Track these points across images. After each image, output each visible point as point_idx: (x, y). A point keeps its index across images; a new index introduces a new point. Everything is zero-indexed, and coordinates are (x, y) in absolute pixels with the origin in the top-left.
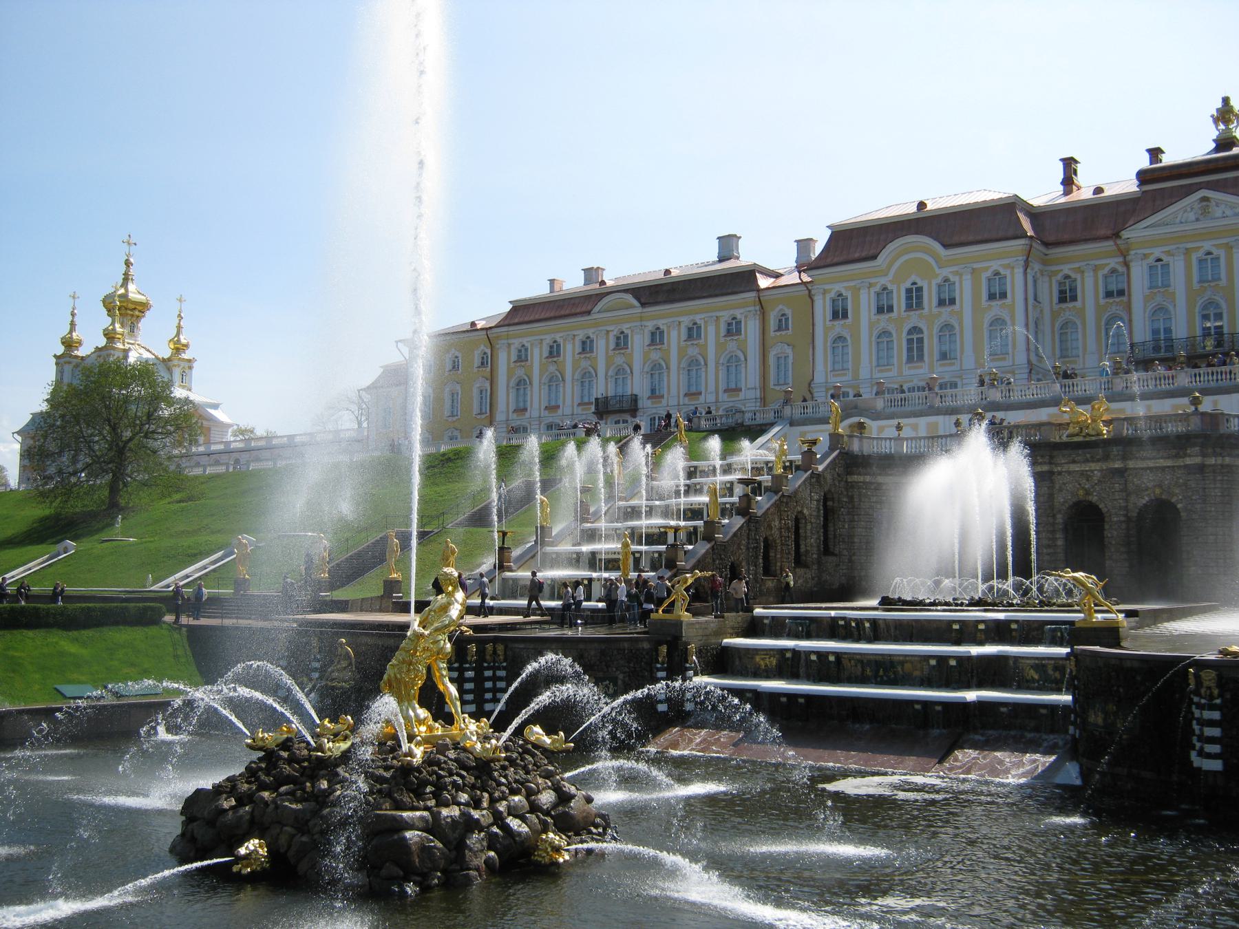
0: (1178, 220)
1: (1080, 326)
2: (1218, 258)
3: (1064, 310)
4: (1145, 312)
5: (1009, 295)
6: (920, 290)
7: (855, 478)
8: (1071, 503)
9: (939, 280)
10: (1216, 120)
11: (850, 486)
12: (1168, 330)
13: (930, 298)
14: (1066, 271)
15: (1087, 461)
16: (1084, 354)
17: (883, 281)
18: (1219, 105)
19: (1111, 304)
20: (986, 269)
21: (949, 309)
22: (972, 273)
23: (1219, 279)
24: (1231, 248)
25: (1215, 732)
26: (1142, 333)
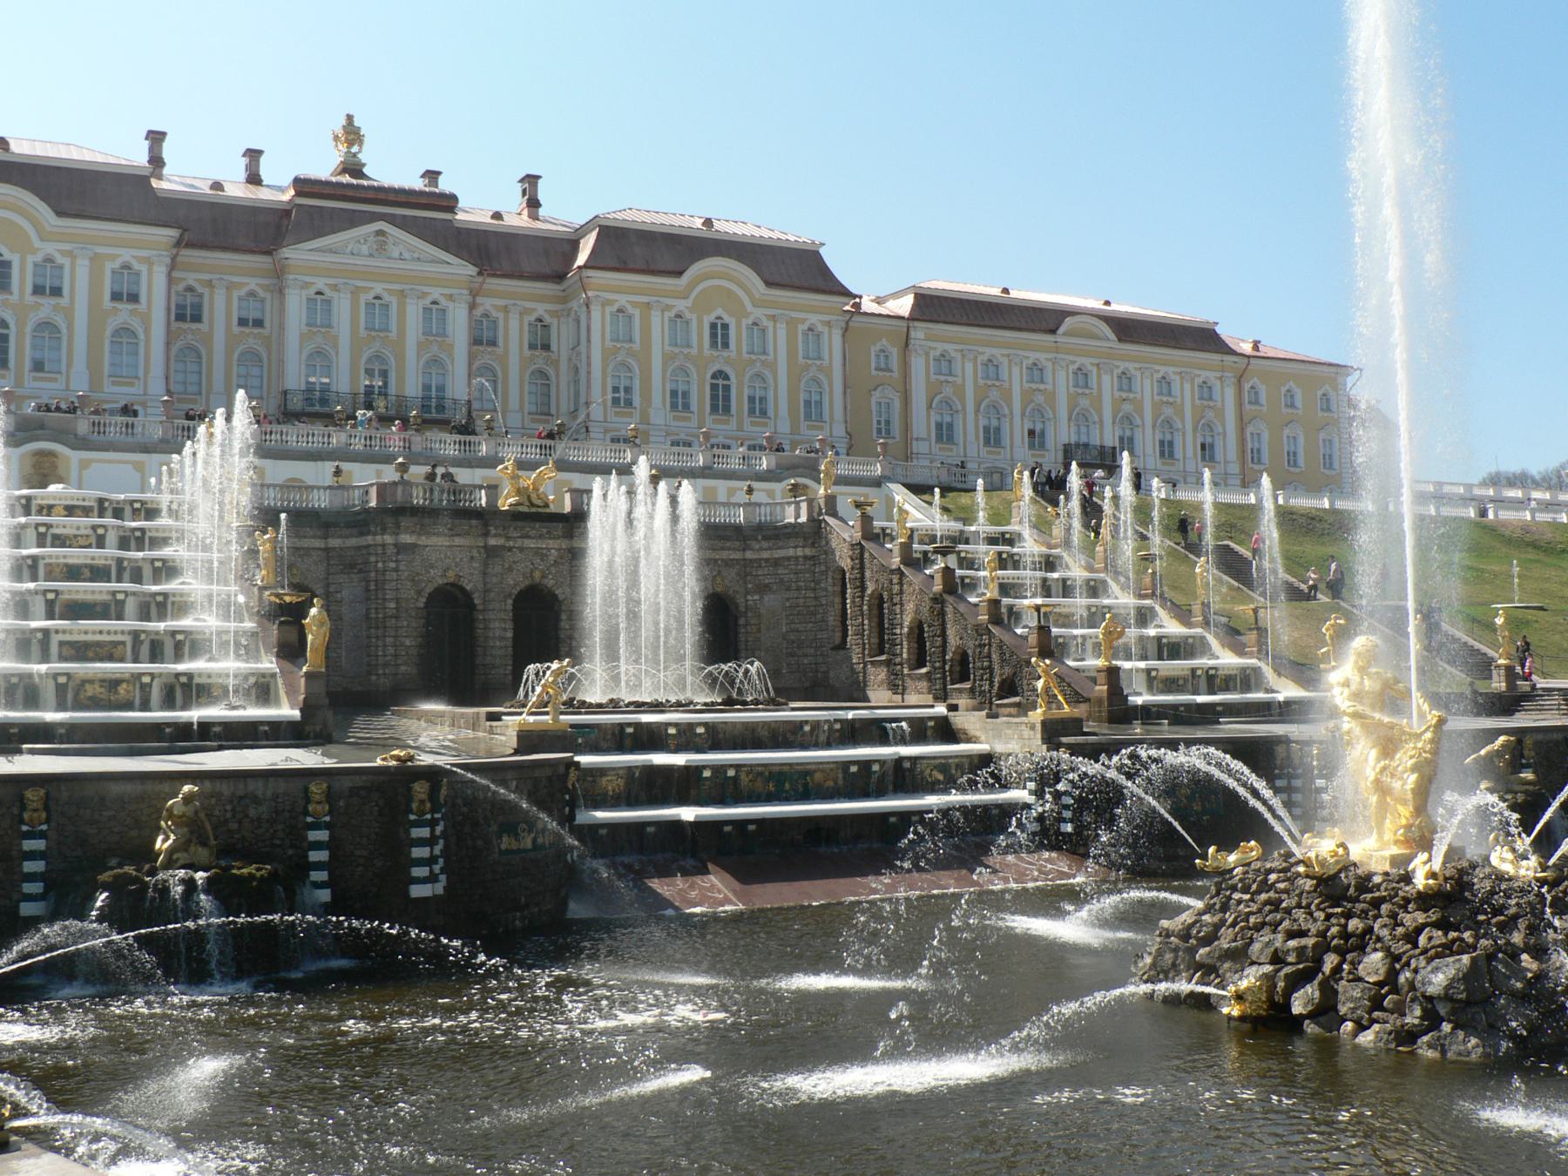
1: (204, 353)
2: (386, 306)
3: (185, 331)
4: (300, 352)
5: (143, 298)
8: (523, 586)
9: (39, 258)
10: (336, 138)
14: (191, 278)
15: (541, 537)
18: (344, 122)
19: (248, 335)
21: (54, 301)
22: (91, 259)
23: (387, 330)
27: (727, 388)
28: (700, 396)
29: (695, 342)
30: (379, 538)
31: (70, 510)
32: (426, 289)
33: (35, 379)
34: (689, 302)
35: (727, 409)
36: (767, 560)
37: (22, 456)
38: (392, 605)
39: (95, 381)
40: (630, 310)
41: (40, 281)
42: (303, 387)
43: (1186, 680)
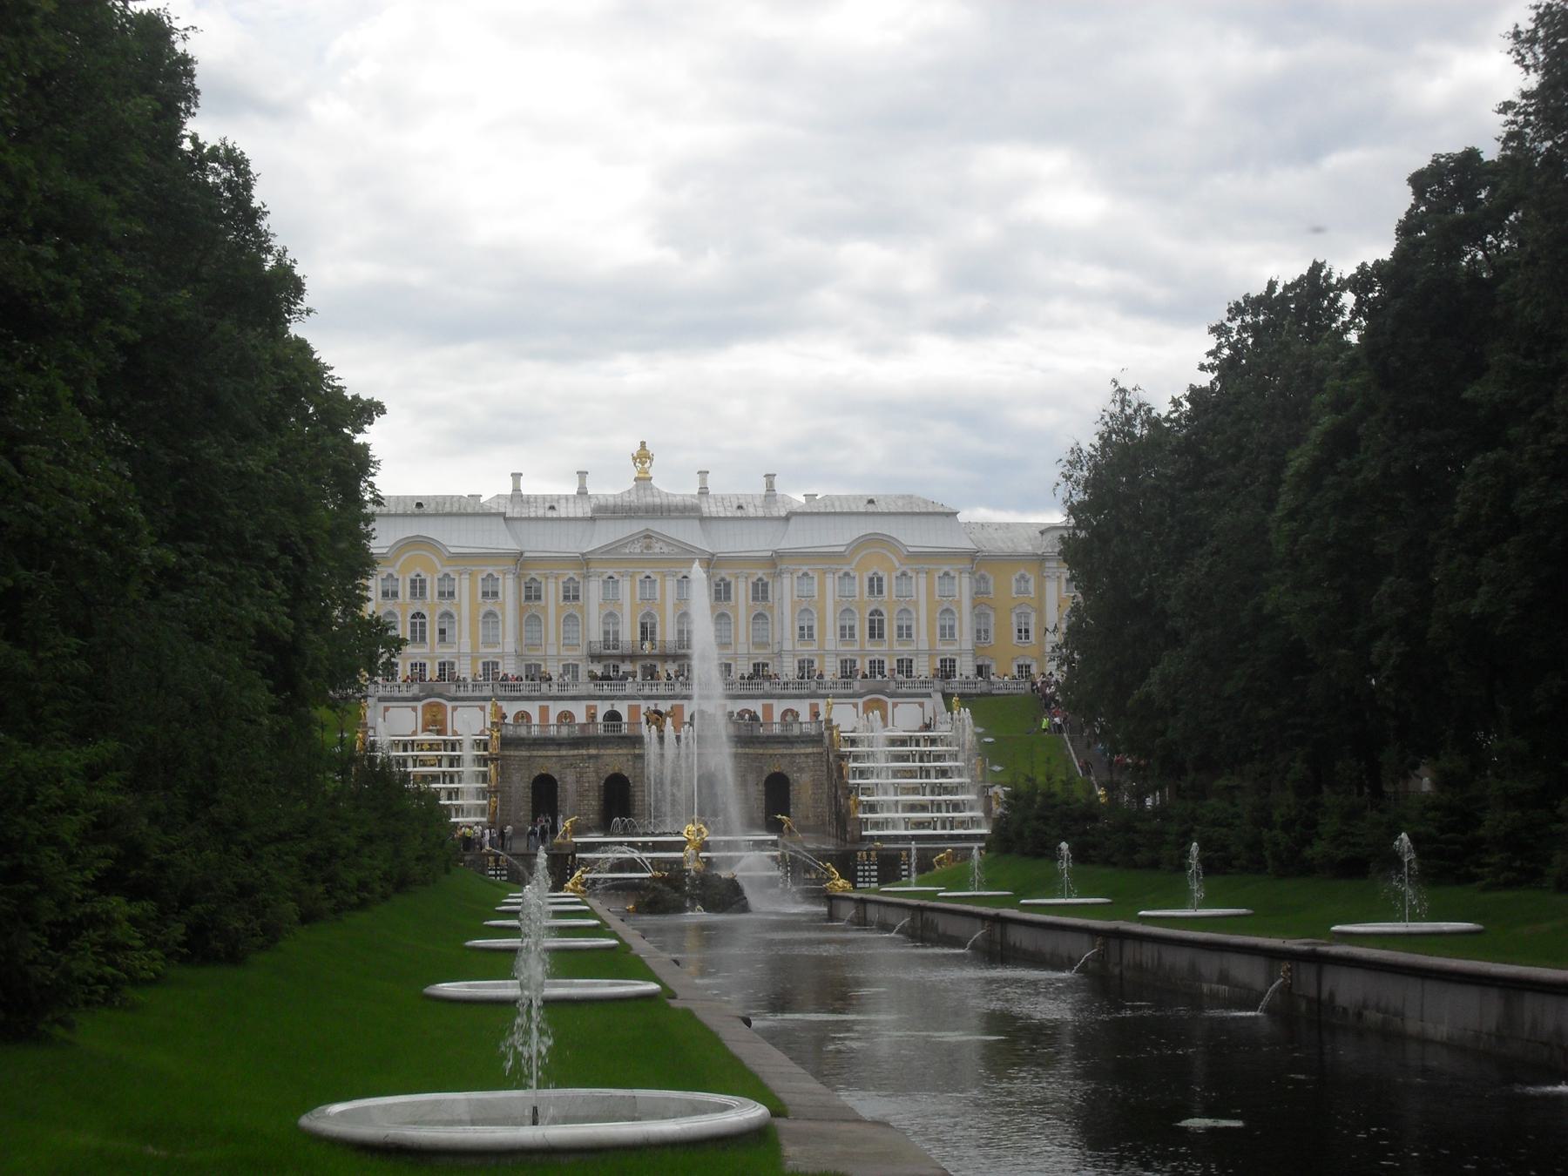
0: (628, 551)
4: (600, 617)
5: (500, 595)
6: (423, 581)
7: (507, 753)
9: (441, 576)
10: (634, 459)
11: (504, 758)
12: (616, 633)
13: (432, 589)
16: (546, 644)
17: (390, 570)
20: (483, 571)
22: (470, 574)
24: (665, 576)
25: (876, 873)
26: (596, 635)
27: (881, 622)
28: (861, 630)
29: (857, 593)
30: (581, 752)
31: (432, 747)
32: (677, 570)
33: (441, 647)
34: (853, 566)
35: (881, 636)
36: (803, 754)
37: (423, 706)
38: (587, 785)
39: (474, 646)
40: (811, 575)
41: (442, 589)
42: (602, 639)
43: (930, 823)
